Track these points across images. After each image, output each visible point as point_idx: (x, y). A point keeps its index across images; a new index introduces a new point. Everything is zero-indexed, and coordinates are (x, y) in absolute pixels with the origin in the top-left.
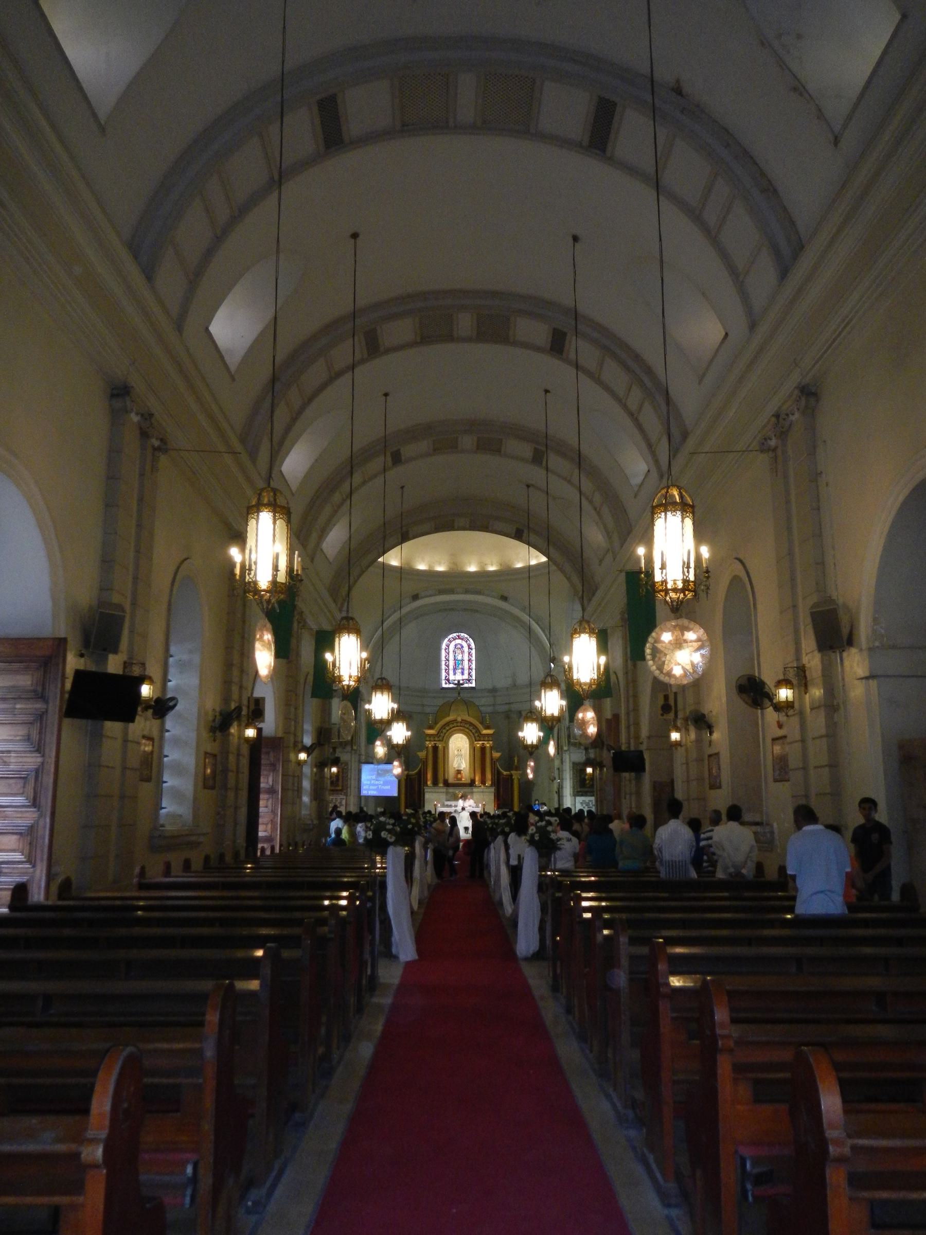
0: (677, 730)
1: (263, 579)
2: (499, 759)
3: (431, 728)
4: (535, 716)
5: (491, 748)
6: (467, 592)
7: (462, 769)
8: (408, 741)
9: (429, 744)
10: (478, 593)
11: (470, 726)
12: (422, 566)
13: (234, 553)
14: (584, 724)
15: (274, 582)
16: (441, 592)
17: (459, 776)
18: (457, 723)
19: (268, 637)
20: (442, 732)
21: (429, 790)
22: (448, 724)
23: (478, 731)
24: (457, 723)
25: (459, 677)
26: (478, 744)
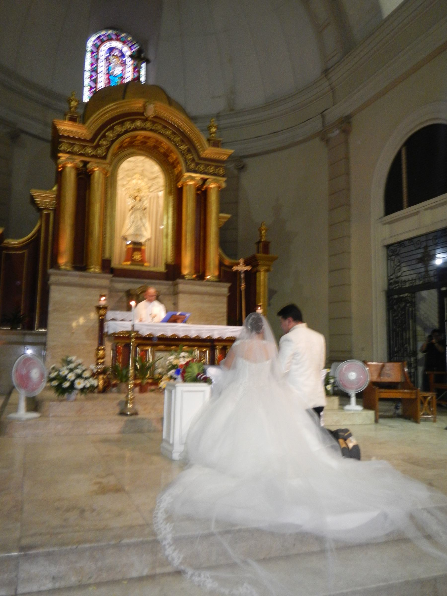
7: (142, 240)
11: (174, 133)
17: (137, 256)
18: (146, 120)
20: (104, 136)
21: (64, 279)
24: (146, 120)
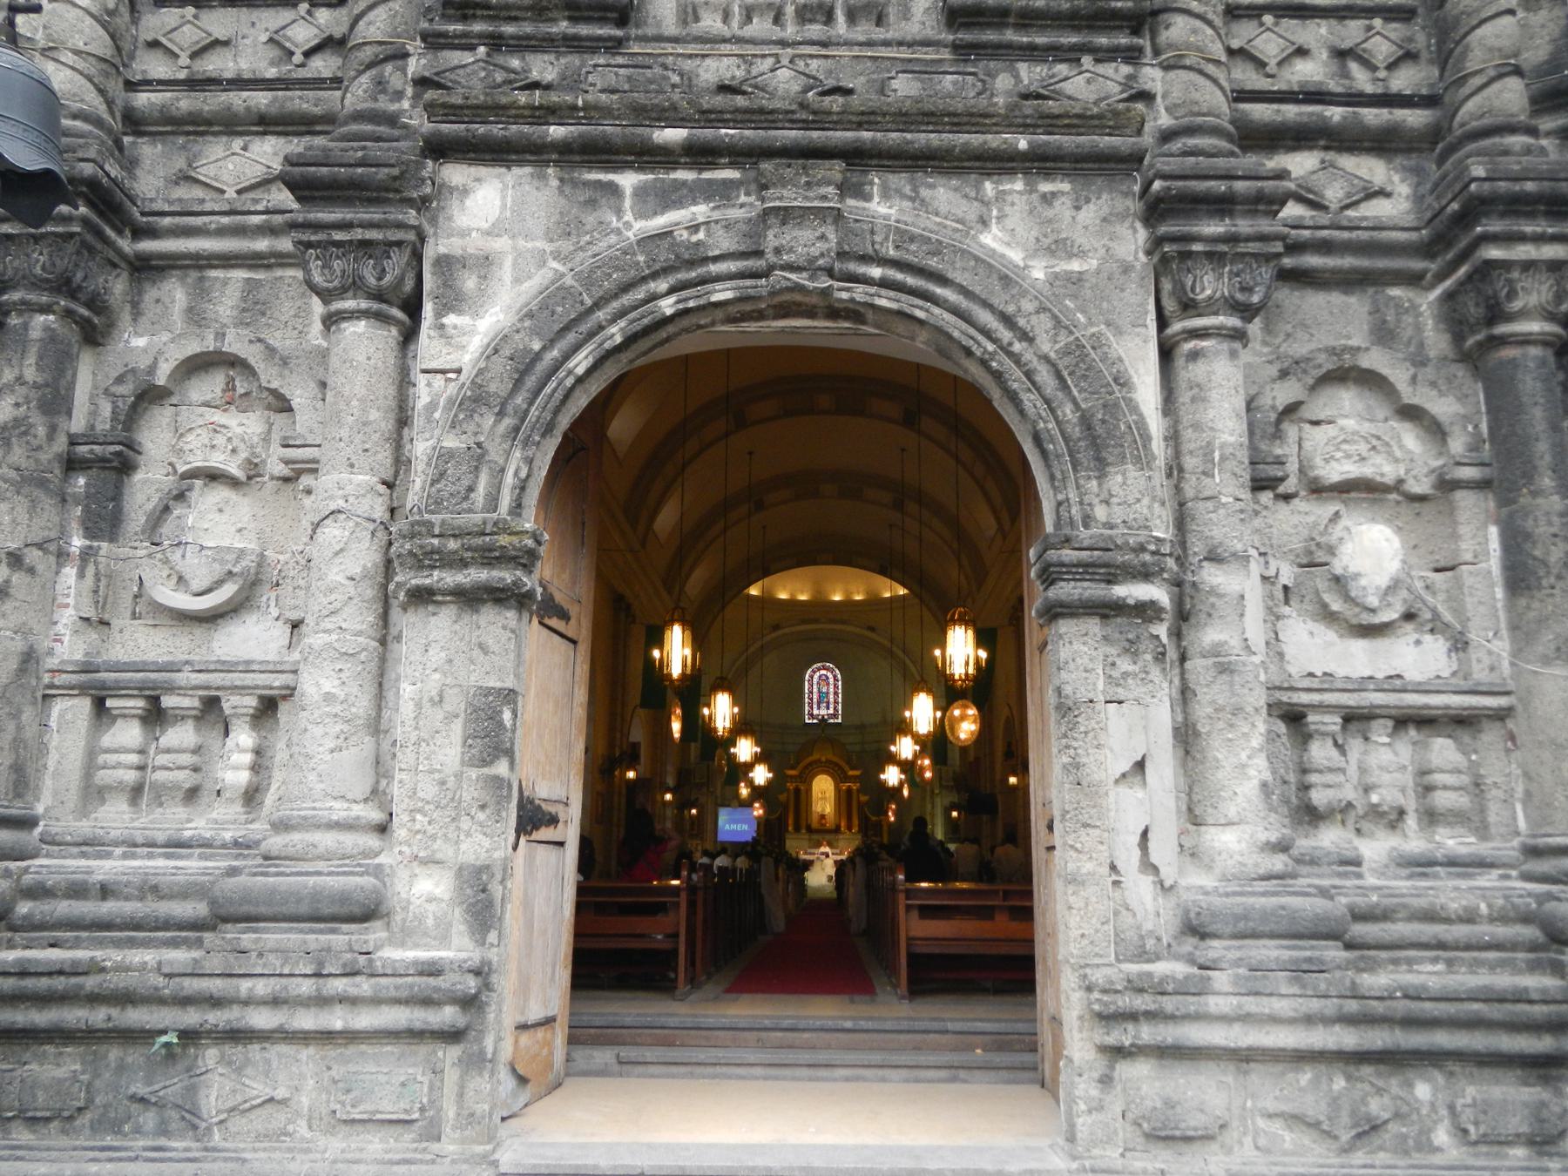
0: (1014, 775)
1: (676, 671)
2: (867, 803)
3: (793, 768)
4: (893, 759)
5: (858, 791)
6: (832, 621)
8: (770, 782)
9: (791, 786)
10: (844, 622)
12: (783, 596)
13: (656, 654)
14: (922, 769)
15: (683, 674)
16: (804, 622)
19: (678, 711)
22: (811, 764)
23: (844, 772)
25: (823, 712)
26: (844, 787)
